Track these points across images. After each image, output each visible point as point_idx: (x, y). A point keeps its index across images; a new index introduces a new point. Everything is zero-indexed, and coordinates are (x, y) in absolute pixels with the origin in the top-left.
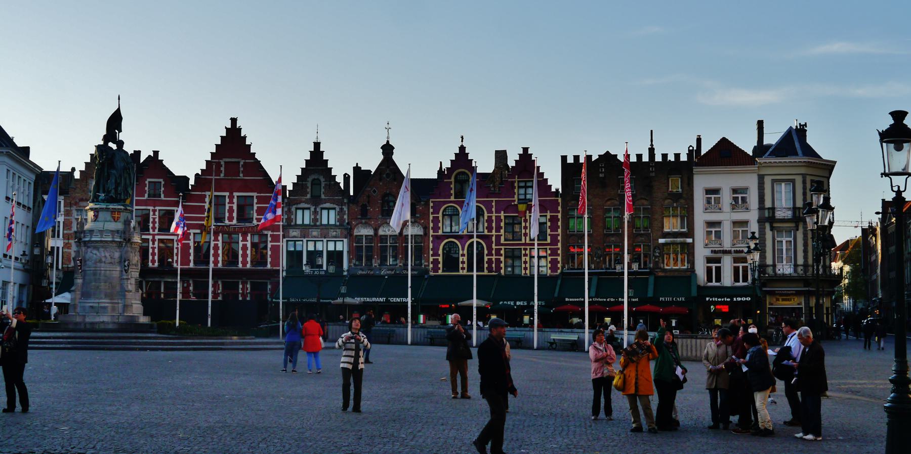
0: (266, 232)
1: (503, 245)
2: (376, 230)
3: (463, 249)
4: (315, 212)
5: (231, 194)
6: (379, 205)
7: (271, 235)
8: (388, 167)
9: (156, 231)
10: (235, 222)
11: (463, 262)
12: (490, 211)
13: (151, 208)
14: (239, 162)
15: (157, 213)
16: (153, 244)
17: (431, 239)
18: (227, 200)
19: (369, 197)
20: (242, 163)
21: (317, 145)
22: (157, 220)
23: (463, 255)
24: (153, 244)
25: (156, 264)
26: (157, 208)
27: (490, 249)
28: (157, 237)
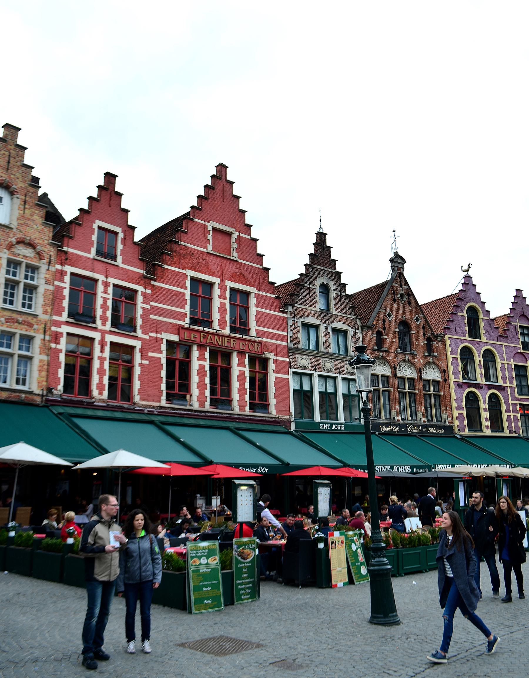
0: (268, 355)
1: (518, 399)
2: (395, 368)
3: (484, 403)
4: (326, 332)
5: (223, 281)
6: (396, 334)
7: (276, 361)
8: (401, 286)
9: (108, 326)
10: (227, 331)
11: (486, 419)
12: (502, 358)
13: (101, 278)
14: (230, 234)
15: (110, 290)
16: (102, 351)
17: (453, 386)
18: (216, 291)
19: (384, 321)
20: (235, 236)
21: (321, 237)
22: (110, 303)
23: (485, 410)
24: (102, 351)
25: (106, 393)
26: (112, 281)
27: (507, 403)
28: (110, 338)
